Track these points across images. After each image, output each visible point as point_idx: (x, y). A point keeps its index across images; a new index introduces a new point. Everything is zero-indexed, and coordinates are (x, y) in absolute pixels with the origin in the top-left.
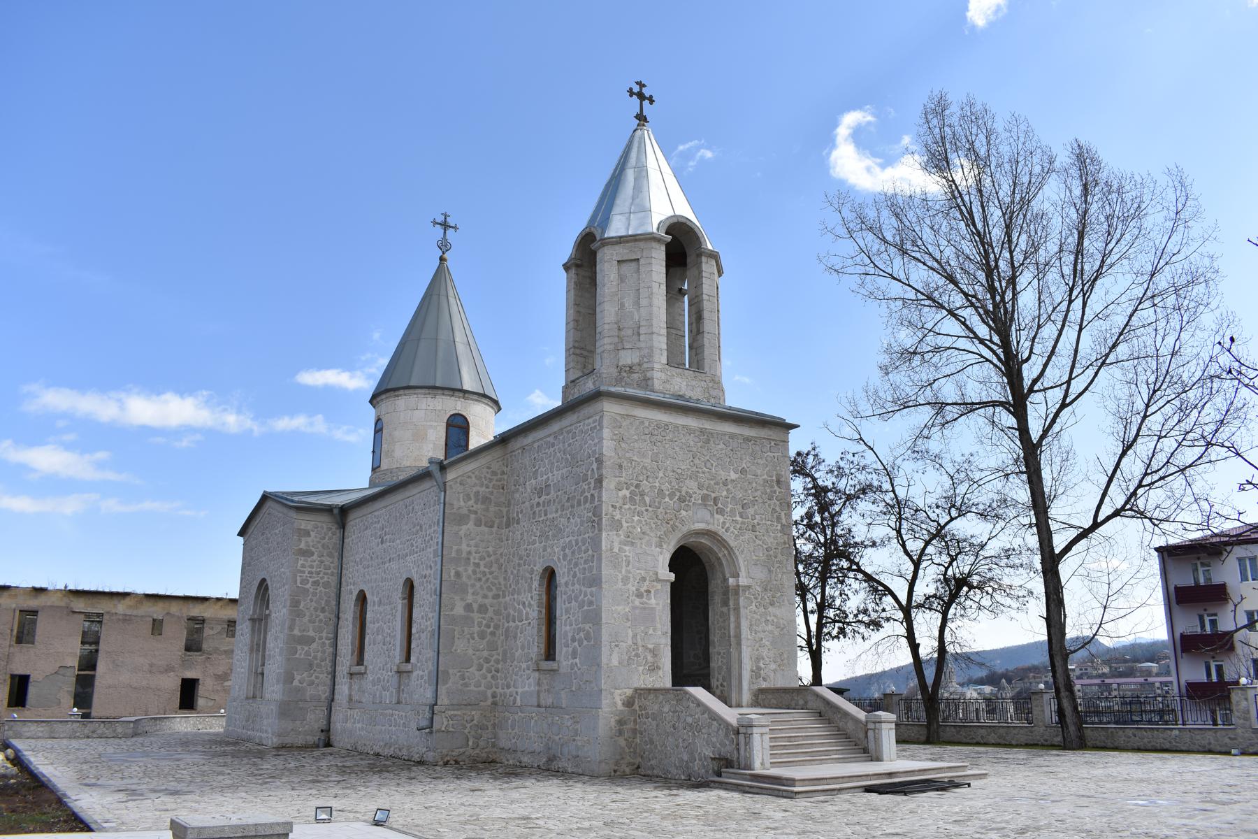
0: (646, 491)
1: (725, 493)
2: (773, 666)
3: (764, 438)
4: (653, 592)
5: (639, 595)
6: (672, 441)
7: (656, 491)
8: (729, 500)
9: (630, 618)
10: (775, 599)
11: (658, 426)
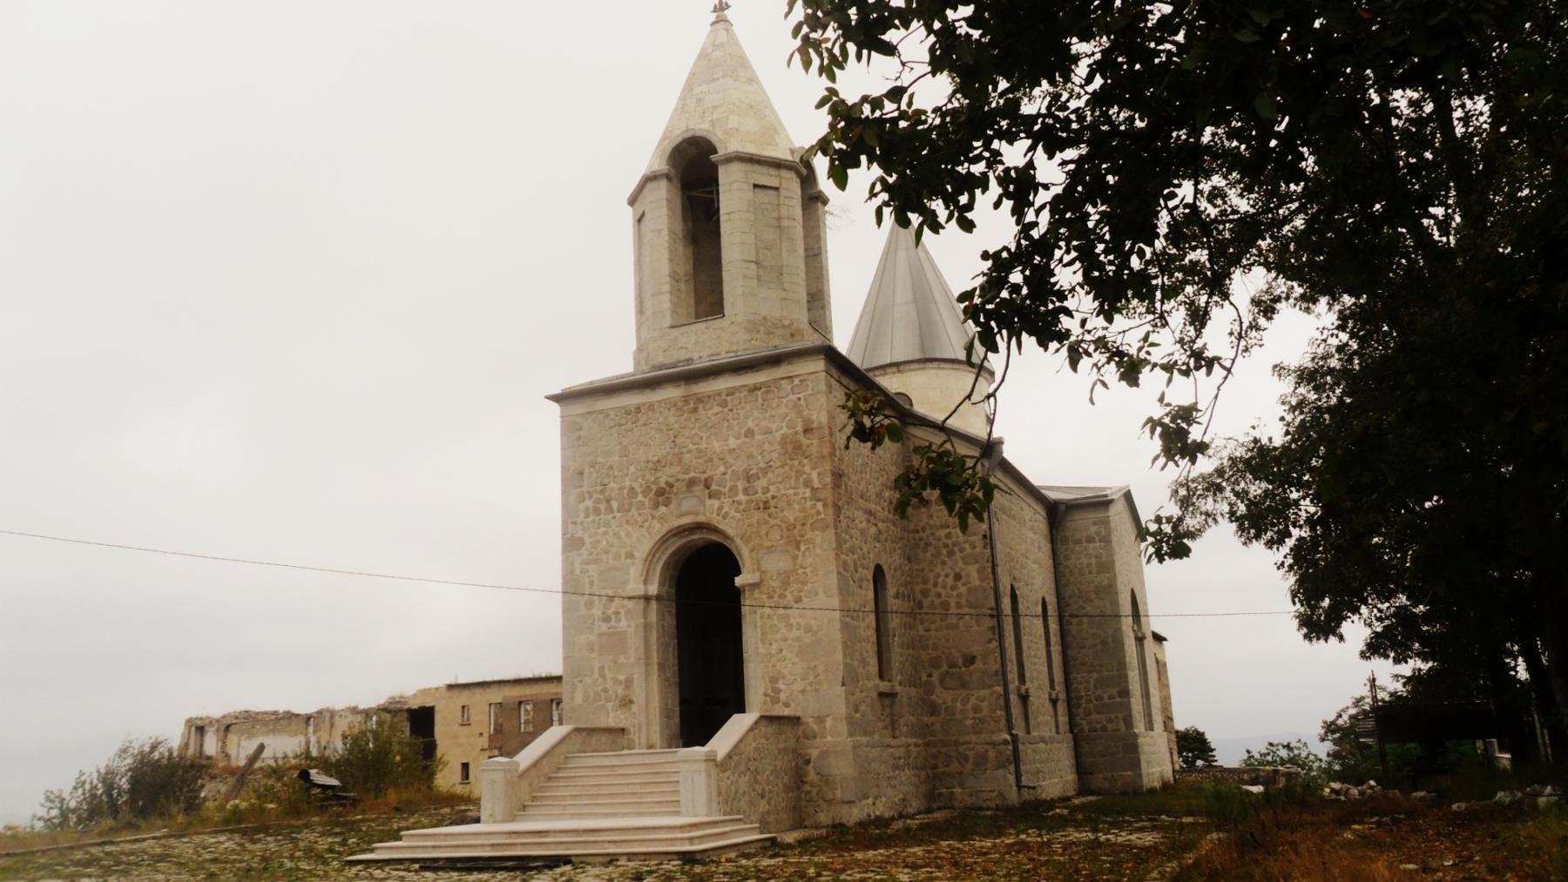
0: (613, 495)
1: (722, 469)
2: (798, 686)
3: (783, 378)
4: (622, 611)
5: (607, 619)
6: (645, 425)
7: (625, 491)
8: (727, 476)
9: (596, 647)
10: (803, 594)
11: (628, 413)
